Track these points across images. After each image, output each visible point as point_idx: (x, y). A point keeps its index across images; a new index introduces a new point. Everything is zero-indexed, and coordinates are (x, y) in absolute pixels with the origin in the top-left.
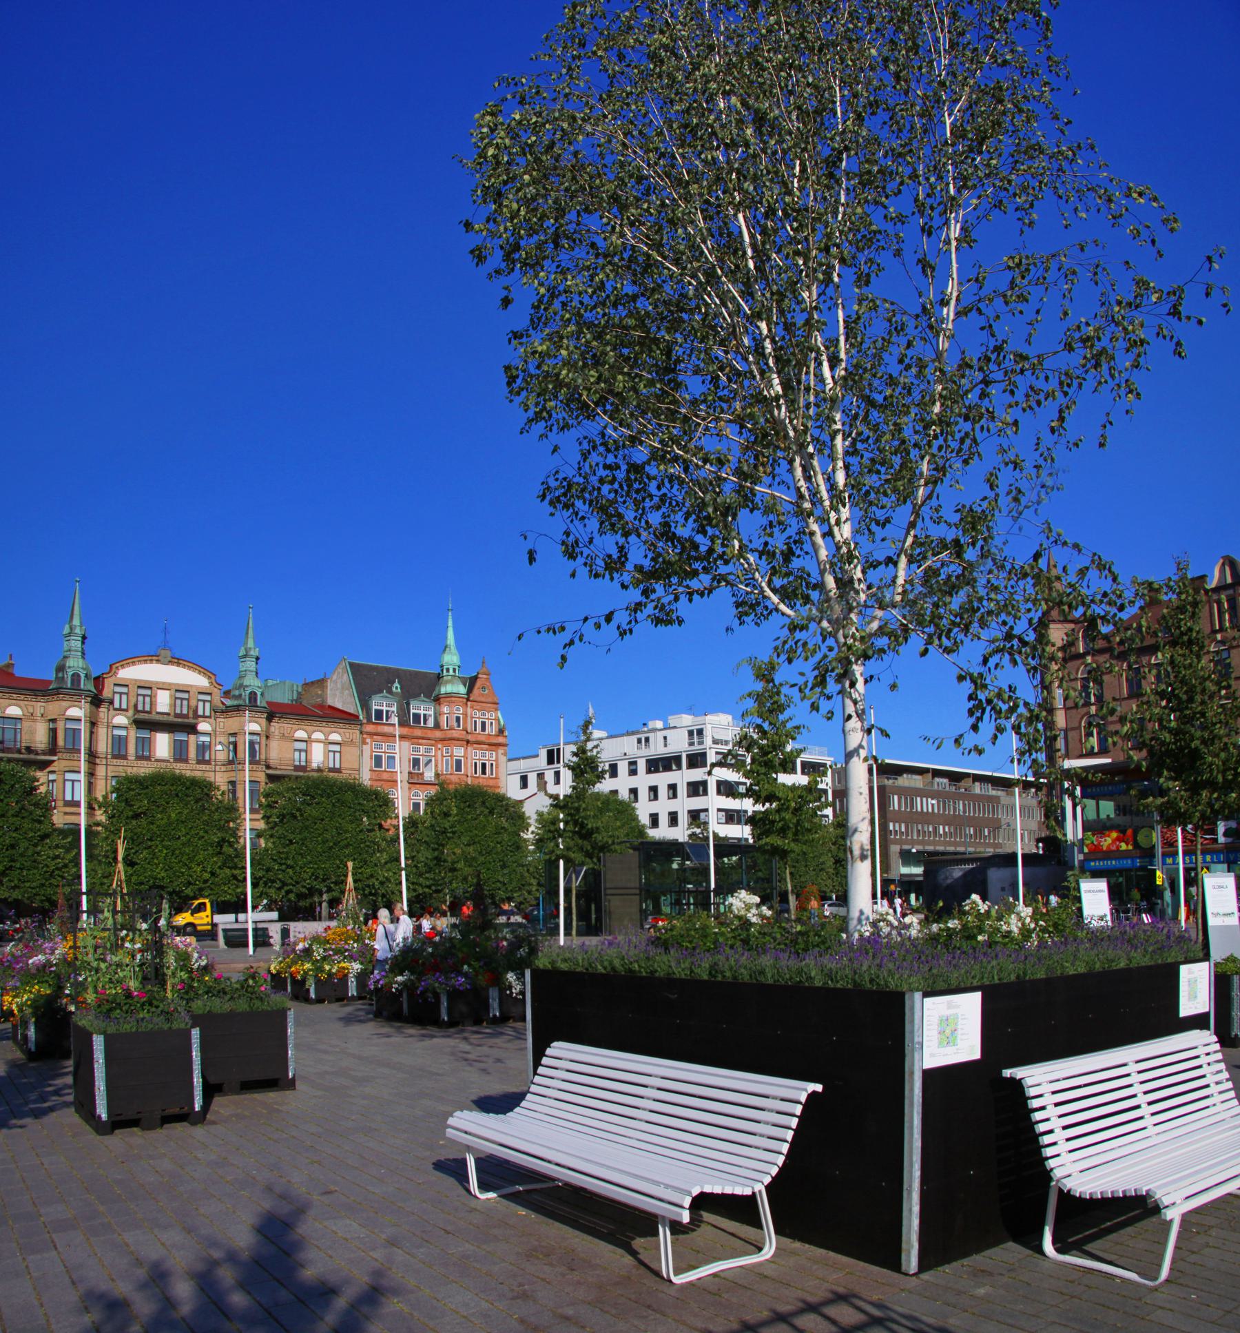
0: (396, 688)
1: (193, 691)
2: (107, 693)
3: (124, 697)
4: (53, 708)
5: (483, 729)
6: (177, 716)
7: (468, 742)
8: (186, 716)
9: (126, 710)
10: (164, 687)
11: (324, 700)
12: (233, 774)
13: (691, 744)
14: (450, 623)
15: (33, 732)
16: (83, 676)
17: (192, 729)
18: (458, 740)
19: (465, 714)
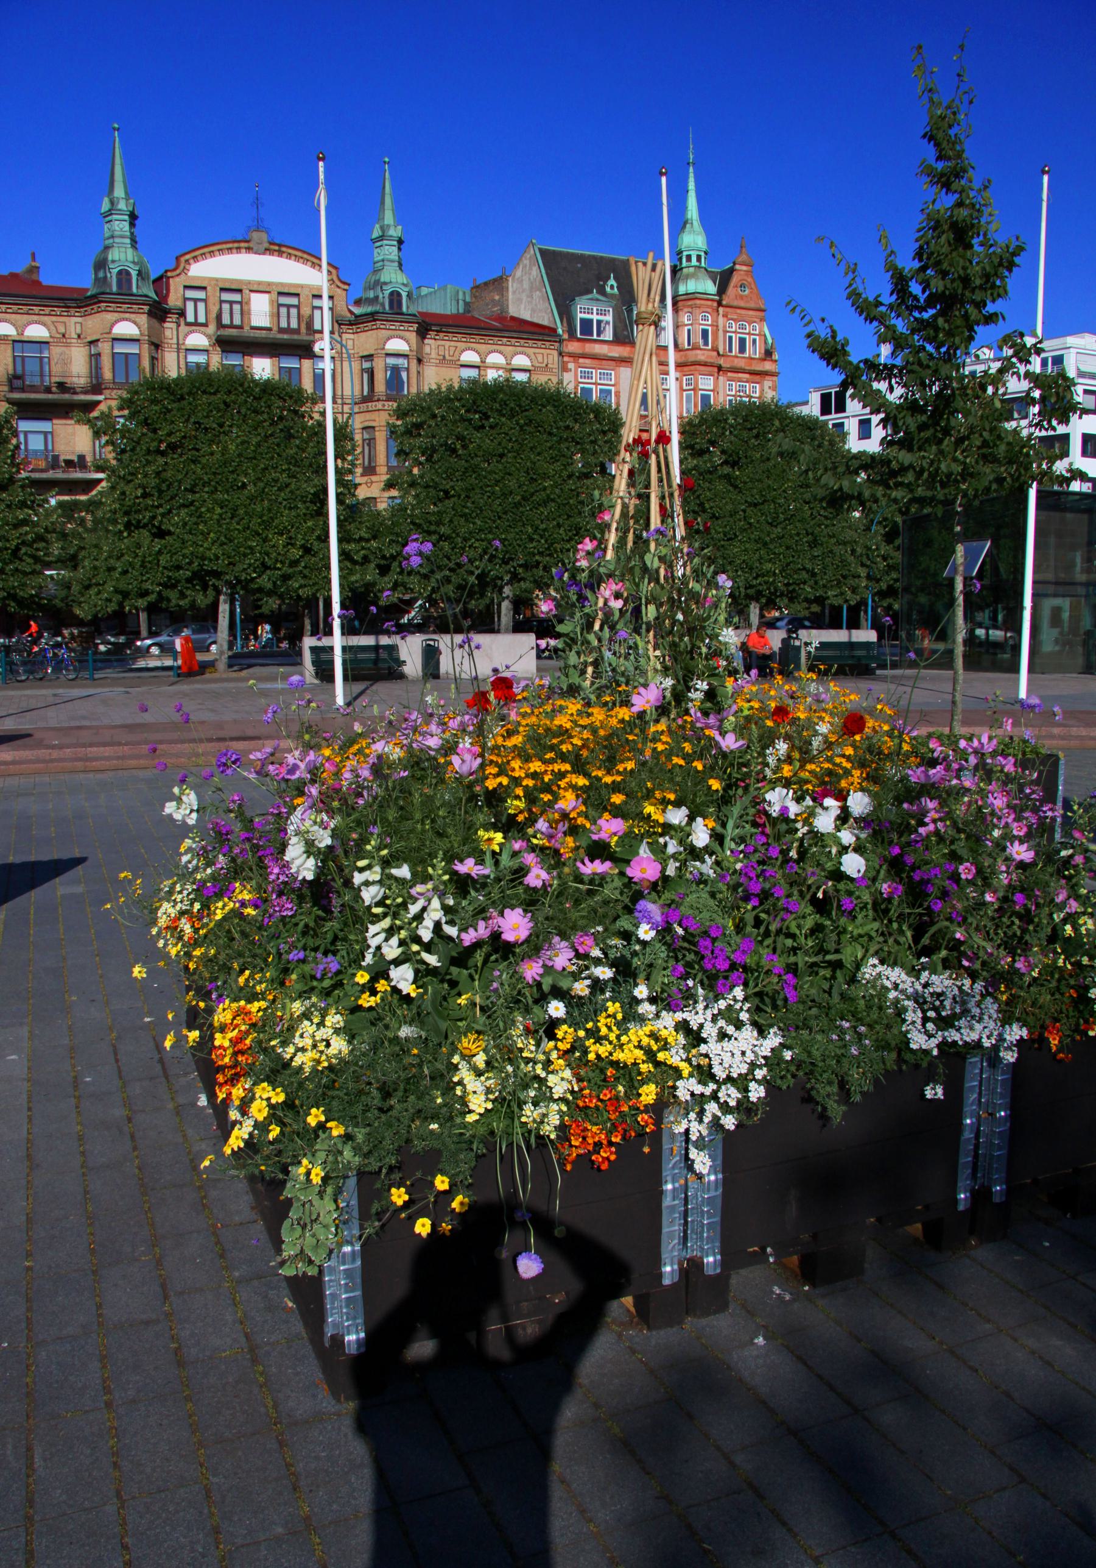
1: (305, 294)
2: (174, 301)
3: (201, 306)
4: (94, 323)
5: (742, 349)
6: (281, 330)
7: (720, 368)
8: (297, 331)
9: (205, 325)
10: (261, 288)
11: (504, 307)
12: (368, 416)
14: (692, 185)
15: (66, 362)
16: (134, 274)
17: (305, 351)
18: (705, 364)
19: (715, 326)
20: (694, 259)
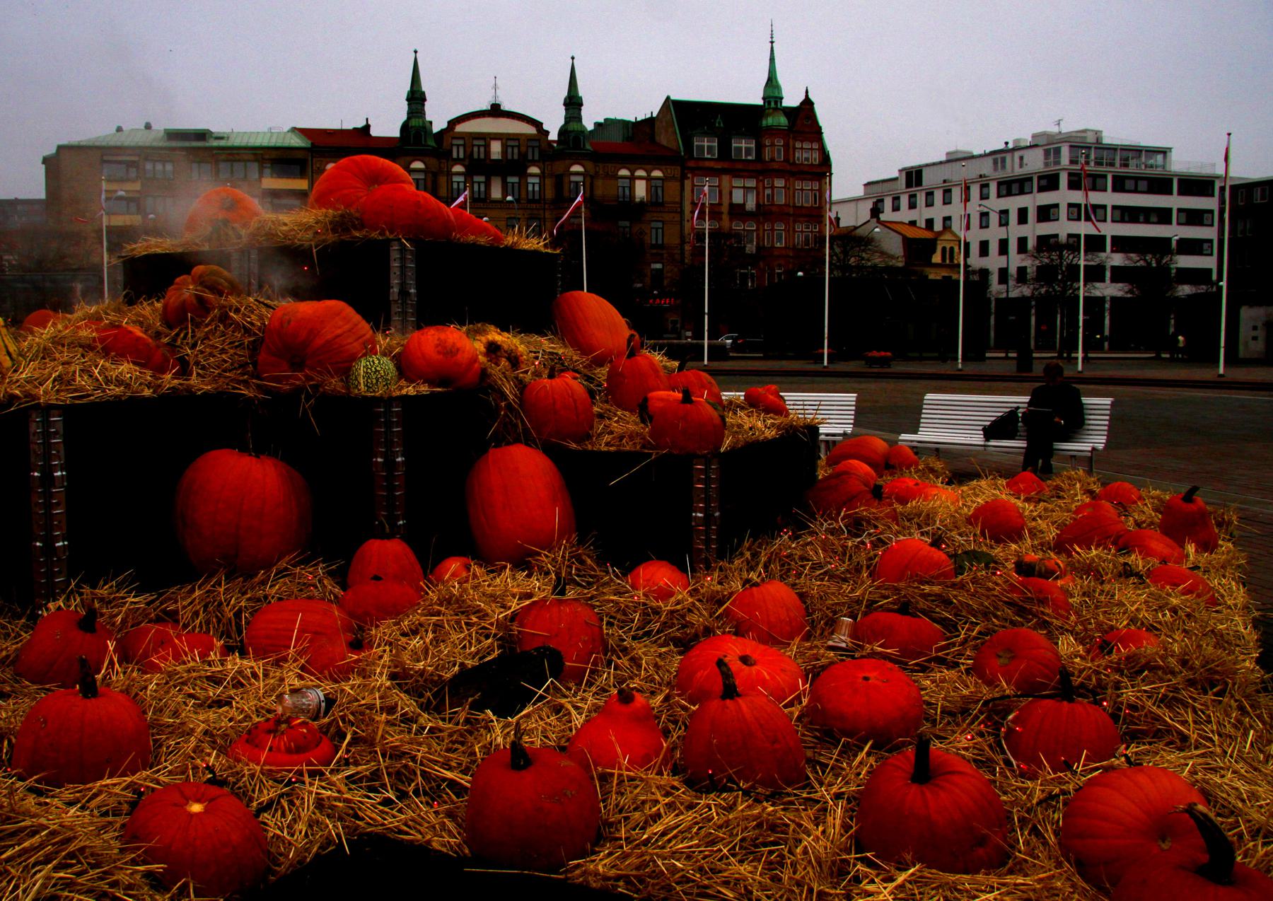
0: (719, 123)
13: (1046, 165)
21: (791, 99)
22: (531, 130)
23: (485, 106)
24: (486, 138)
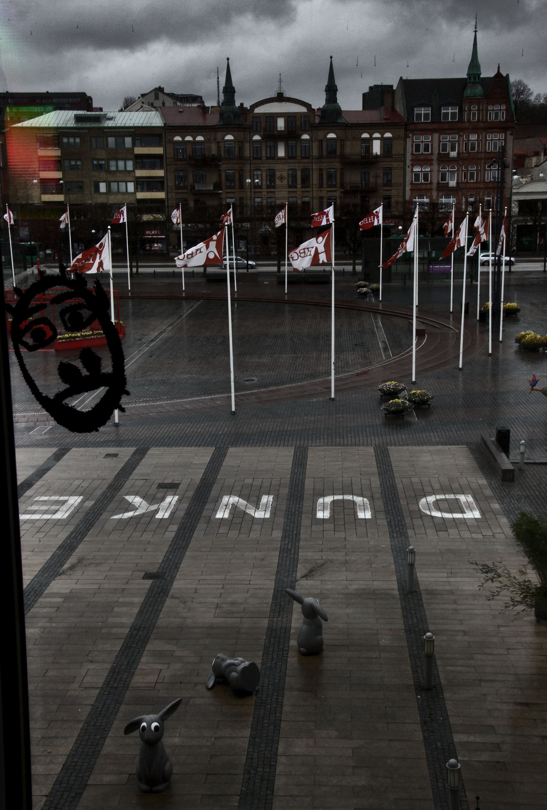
20: (472, 79)
21: (487, 73)
22: (303, 110)
23: (274, 95)
24: (273, 117)
